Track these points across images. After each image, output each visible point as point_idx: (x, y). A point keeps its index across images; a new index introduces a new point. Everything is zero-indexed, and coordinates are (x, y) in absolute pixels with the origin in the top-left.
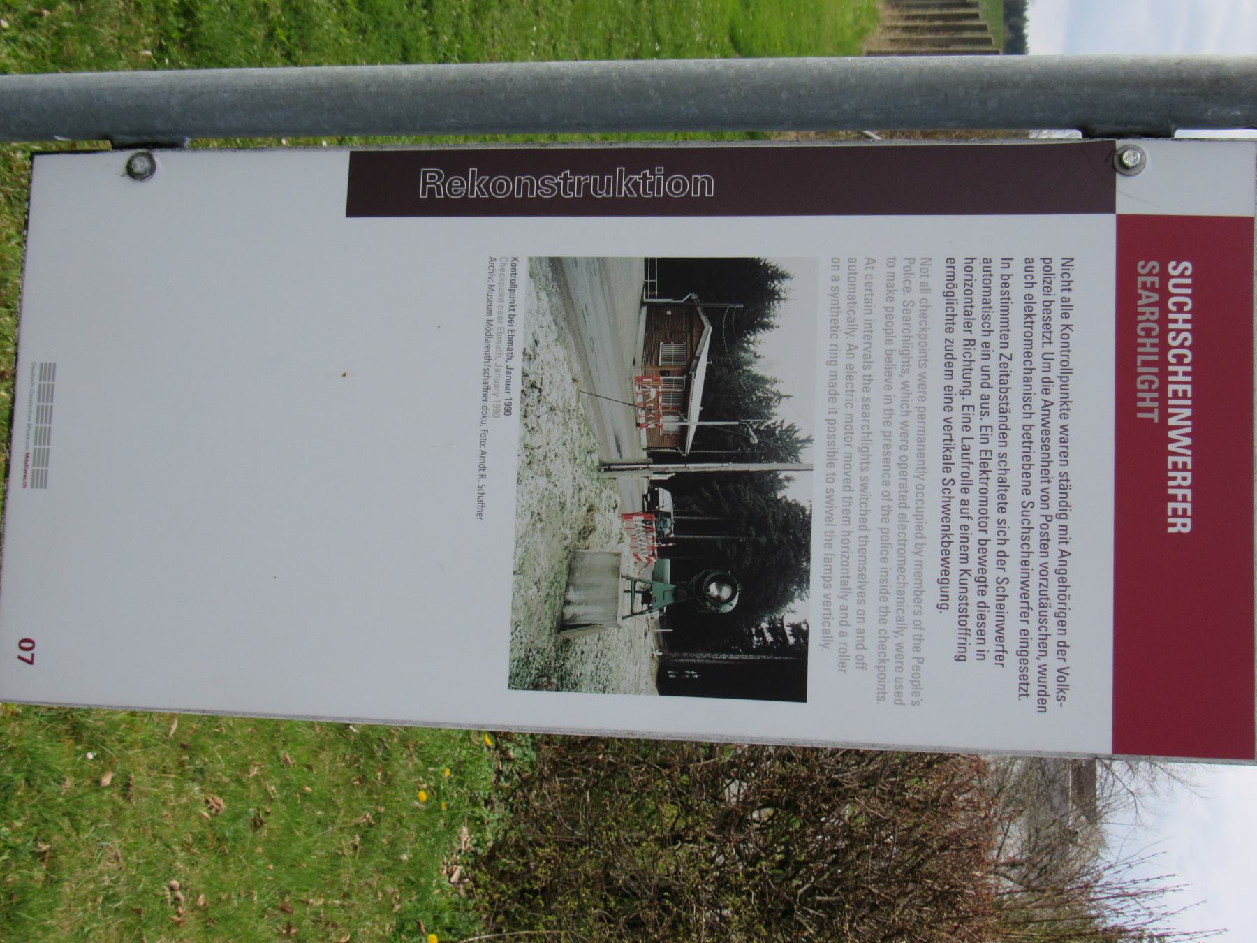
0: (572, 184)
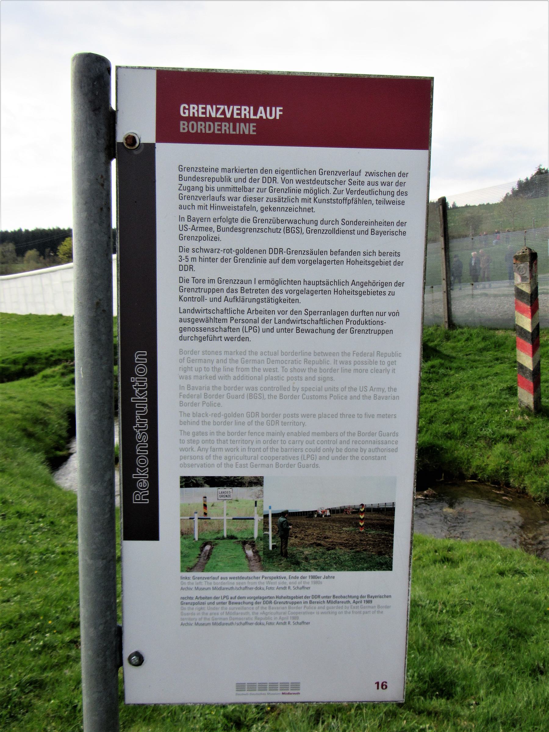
0: (141, 425)
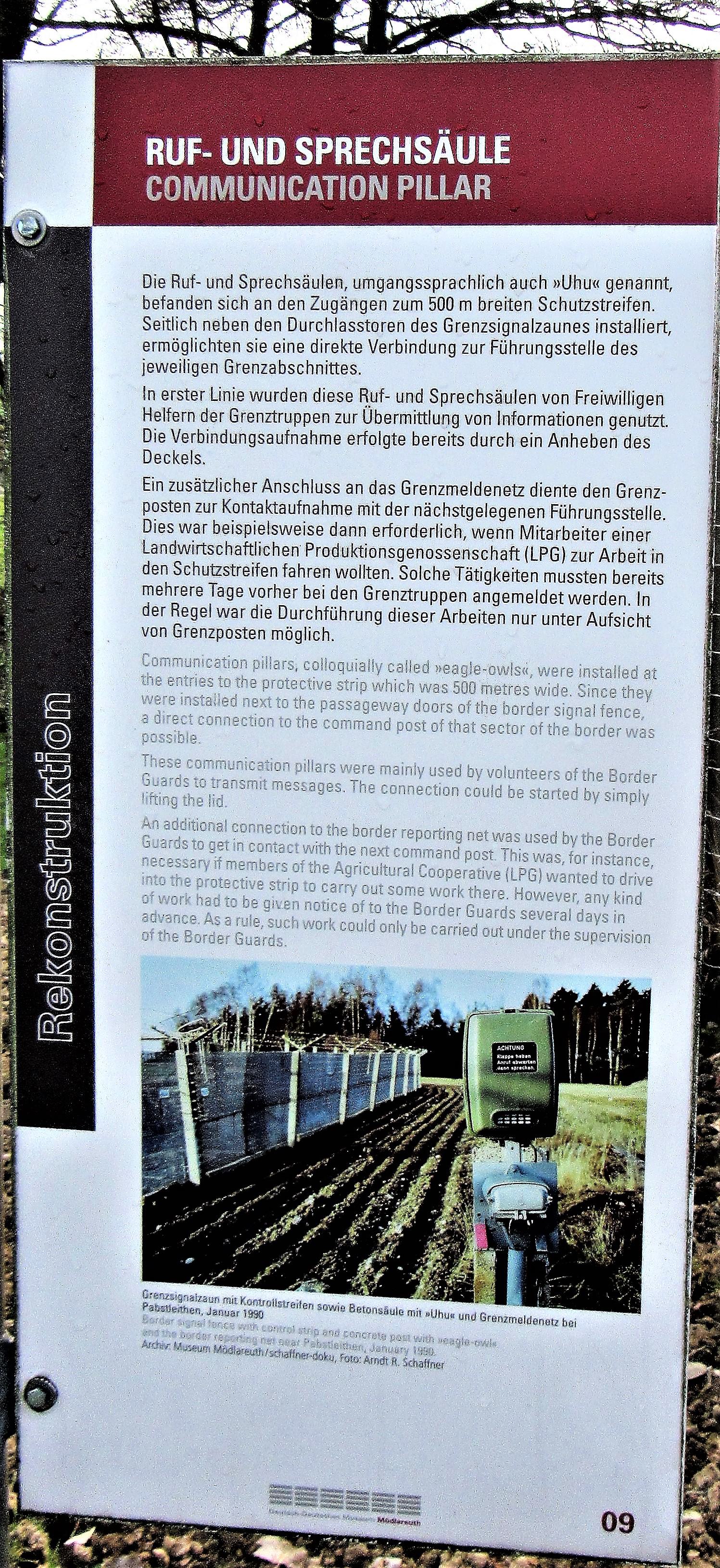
0: (57, 860)
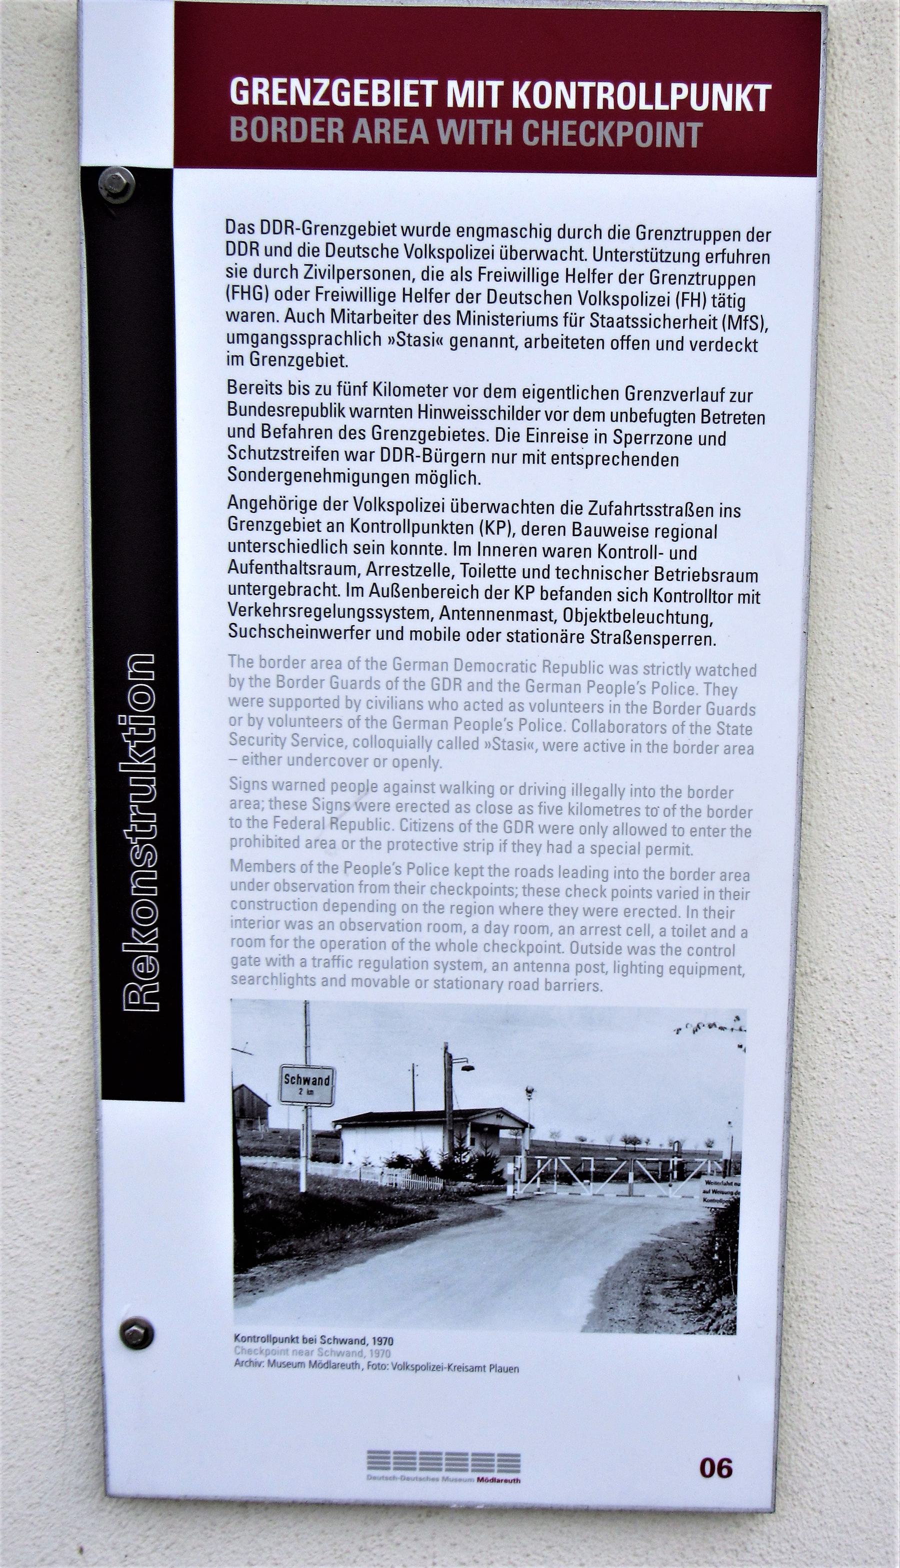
0: (141, 826)
